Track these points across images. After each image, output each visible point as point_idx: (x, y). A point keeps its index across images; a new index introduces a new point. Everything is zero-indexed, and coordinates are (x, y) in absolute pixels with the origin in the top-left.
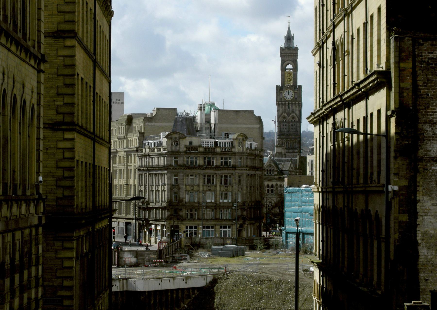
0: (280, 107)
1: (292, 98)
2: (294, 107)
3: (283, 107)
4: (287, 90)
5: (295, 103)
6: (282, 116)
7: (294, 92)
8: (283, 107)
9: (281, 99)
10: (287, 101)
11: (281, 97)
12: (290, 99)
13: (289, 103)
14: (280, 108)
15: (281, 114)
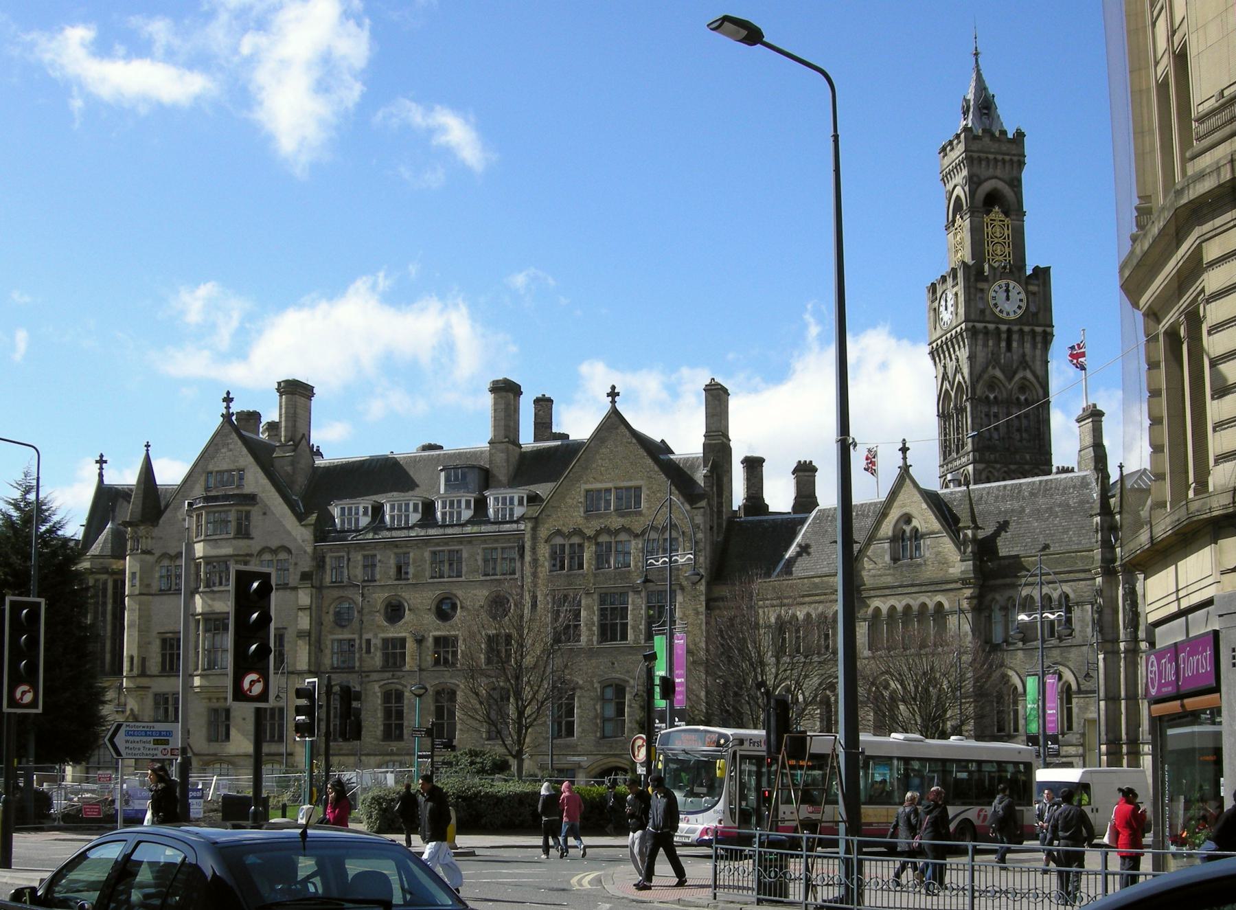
0: (980, 342)
1: (1020, 312)
2: (1028, 346)
4: (1003, 282)
5: (1033, 332)
6: (986, 376)
7: (1027, 292)
8: (991, 343)
9: (983, 312)
10: (1004, 322)
11: (981, 306)
12: (1012, 316)
13: (1009, 331)
14: (979, 348)
15: (985, 370)
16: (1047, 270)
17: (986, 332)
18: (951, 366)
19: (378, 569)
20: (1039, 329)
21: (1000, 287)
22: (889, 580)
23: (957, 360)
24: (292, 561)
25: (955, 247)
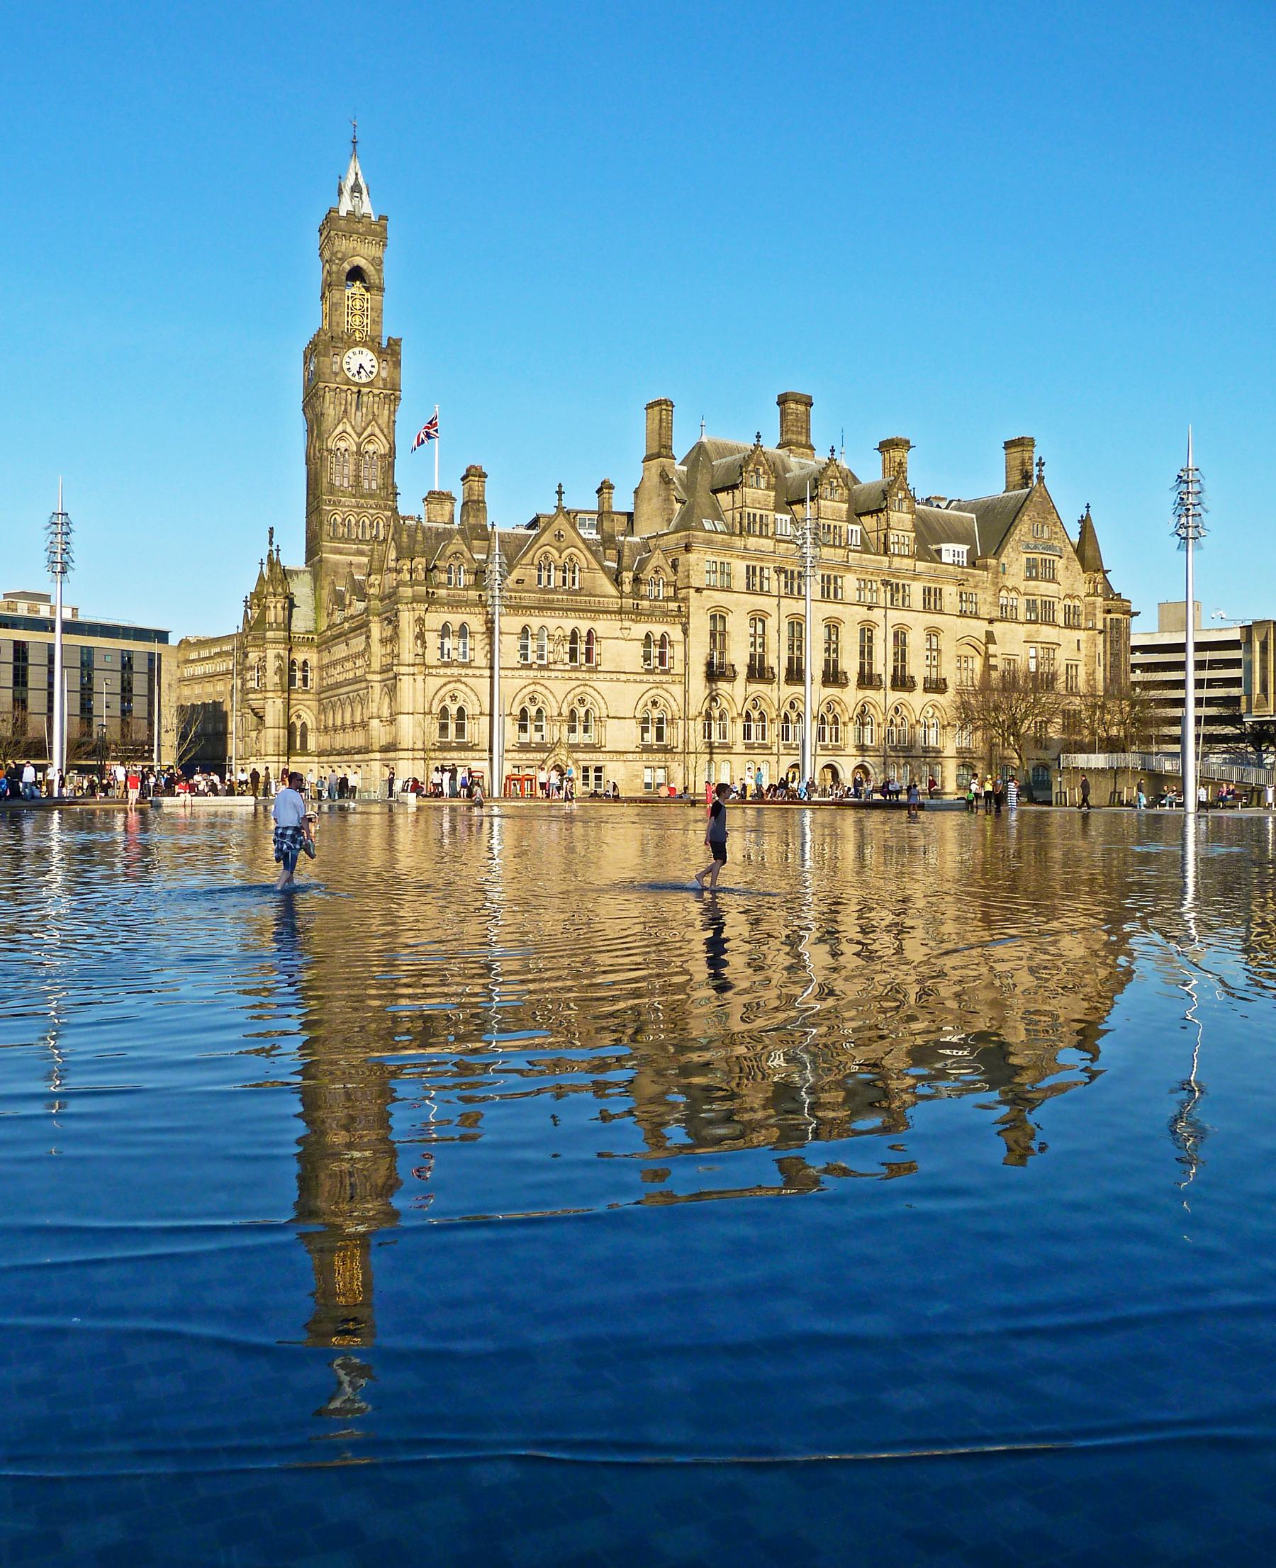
10: (356, 384)
12: (364, 380)
13: (359, 392)
16: (397, 342)
21: (354, 353)
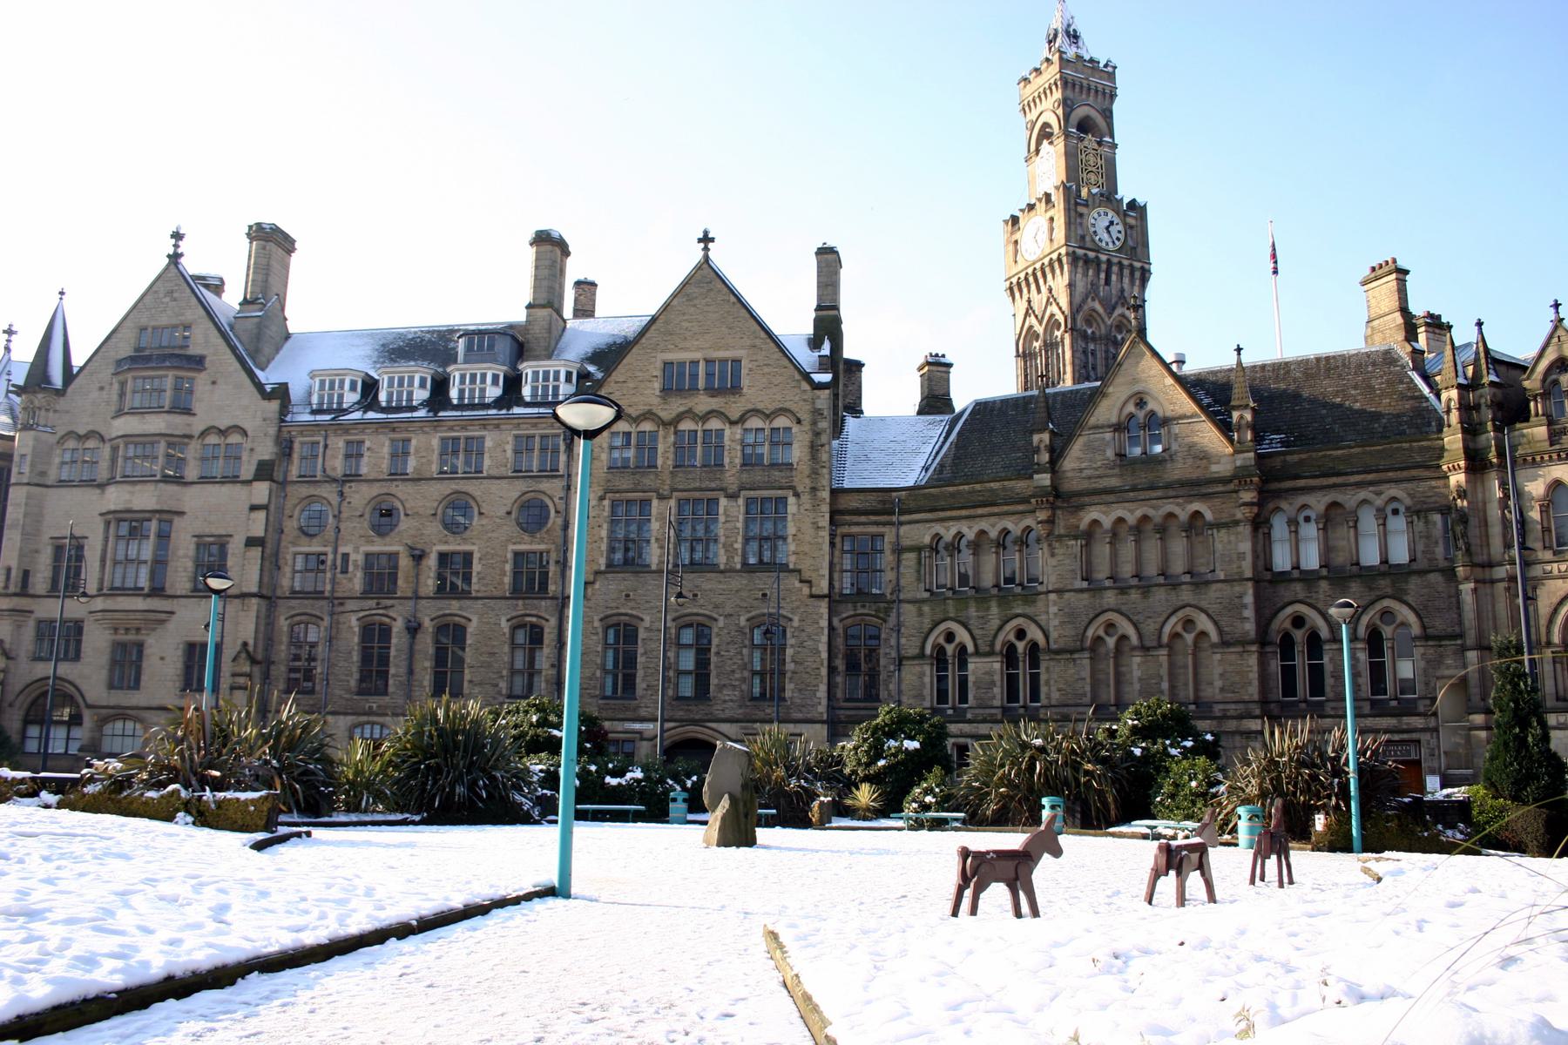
0: (1080, 270)
2: (1126, 280)
3: (1091, 272)
6: (1085, 307)
7: (1125, 224)
8: (1091, 272)
9: (1083, 237)
11: (1080, 232)
13: (1109, 262)
14: (1079, 276)
15: (1084, 301)
17: (1087, 261)
18: (1039, 301)
19: (365, 460)
20: (1137, 265)
22: (1114, 482)
23: (1050, 290)
24: (248, 445)
25: (1051, 167)
